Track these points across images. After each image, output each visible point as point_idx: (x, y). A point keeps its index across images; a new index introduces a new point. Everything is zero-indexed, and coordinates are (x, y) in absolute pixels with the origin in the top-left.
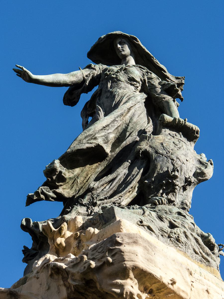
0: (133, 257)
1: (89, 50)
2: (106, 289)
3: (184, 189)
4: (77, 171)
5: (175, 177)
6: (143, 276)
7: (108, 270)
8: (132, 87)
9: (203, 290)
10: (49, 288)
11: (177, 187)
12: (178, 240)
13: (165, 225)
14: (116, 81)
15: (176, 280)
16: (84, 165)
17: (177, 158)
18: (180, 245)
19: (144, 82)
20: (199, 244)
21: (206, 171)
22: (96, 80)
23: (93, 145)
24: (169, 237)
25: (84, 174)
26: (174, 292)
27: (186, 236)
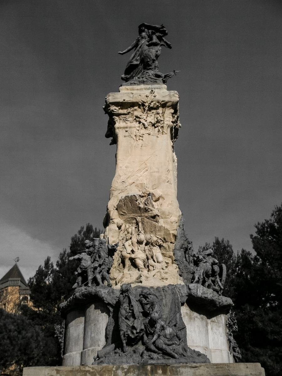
0: (109, 100)
3: (153, 62)
4: (132, 73)
5: (149, 61)
8: (144, 39)
9: (138, 96)
11: (150, 64)
15: (125, 99)
16: (133, 71)
17: (149, 55)
18: (145, 83)
19: (148, 35)
20: (152, 79)
23: (129, 65)
26: (125, 103)
27: (147, 79)
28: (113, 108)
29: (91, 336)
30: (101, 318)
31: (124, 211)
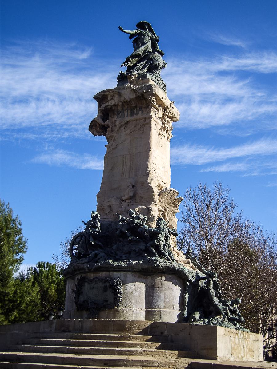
0: (155, 91)
1: (136, 24)
2: (147, 98)
3: (159, 69)
4: (134, 59)
6: (156, 96)
7: (148, 93)
10: (130, 94)
12: (159, 84)
13: (156, 80)
14: (144, 36)
15: (163, 98)
21: (165, 66)
22: (139, 34)
24: (157, 83)
25: (135, 61)
28: (153, 98)
29: (164, 300)
30: (175, 288)
31: (163, 199)
